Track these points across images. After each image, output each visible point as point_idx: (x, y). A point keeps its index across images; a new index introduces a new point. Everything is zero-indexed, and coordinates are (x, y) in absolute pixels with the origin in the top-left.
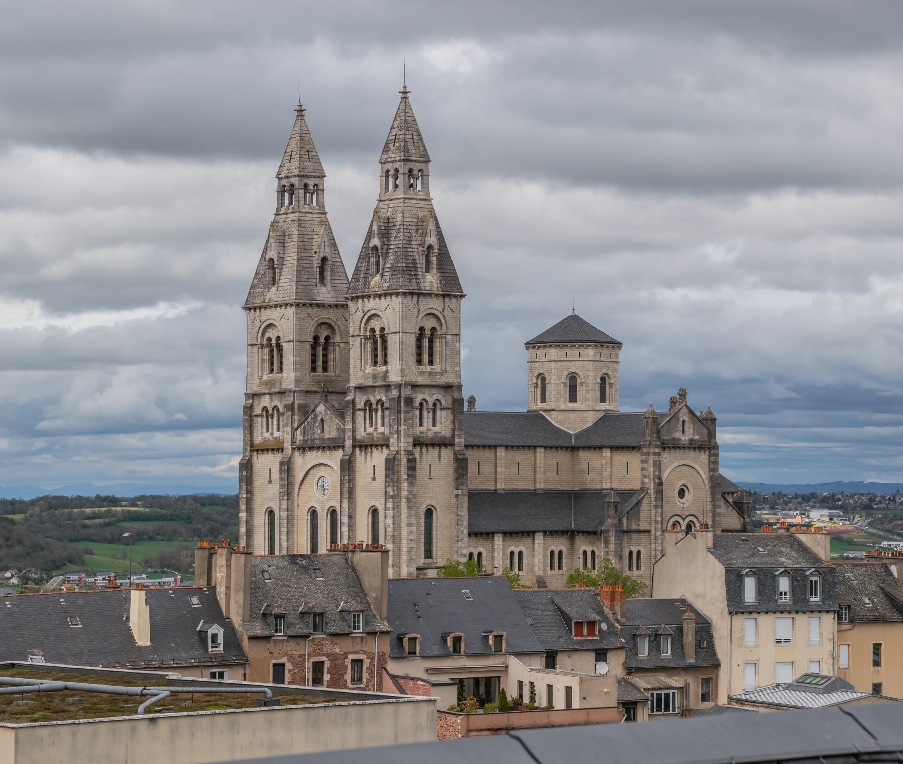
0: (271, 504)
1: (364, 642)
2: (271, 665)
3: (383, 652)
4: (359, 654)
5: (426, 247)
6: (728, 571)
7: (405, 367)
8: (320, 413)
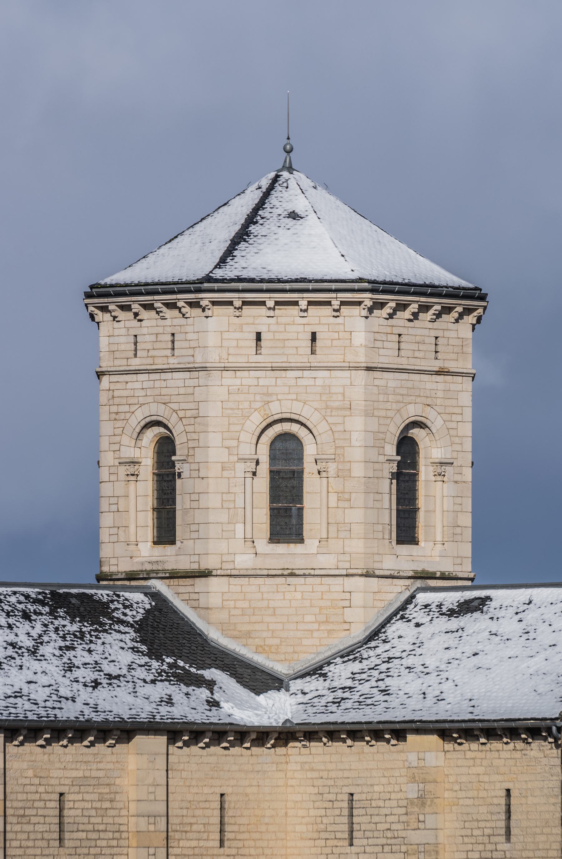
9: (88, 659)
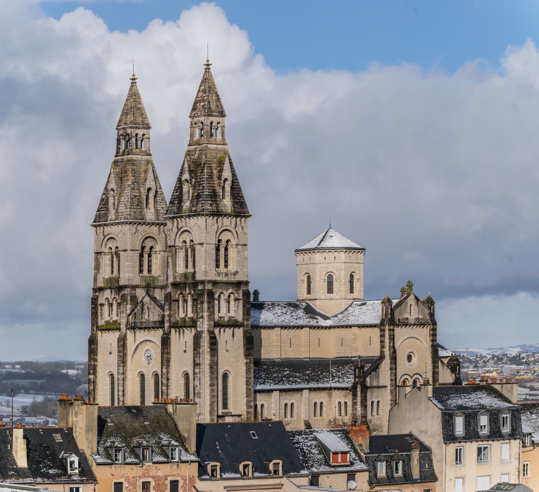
0: (111, 370)
1: (179, 468)
2: (113, 484)
3: (193, 476)
4: (176, 476)
5: (223, 180)
6: (444, 414)
7: (208, 269)
8: (147, 303)
9: (295, 315)
